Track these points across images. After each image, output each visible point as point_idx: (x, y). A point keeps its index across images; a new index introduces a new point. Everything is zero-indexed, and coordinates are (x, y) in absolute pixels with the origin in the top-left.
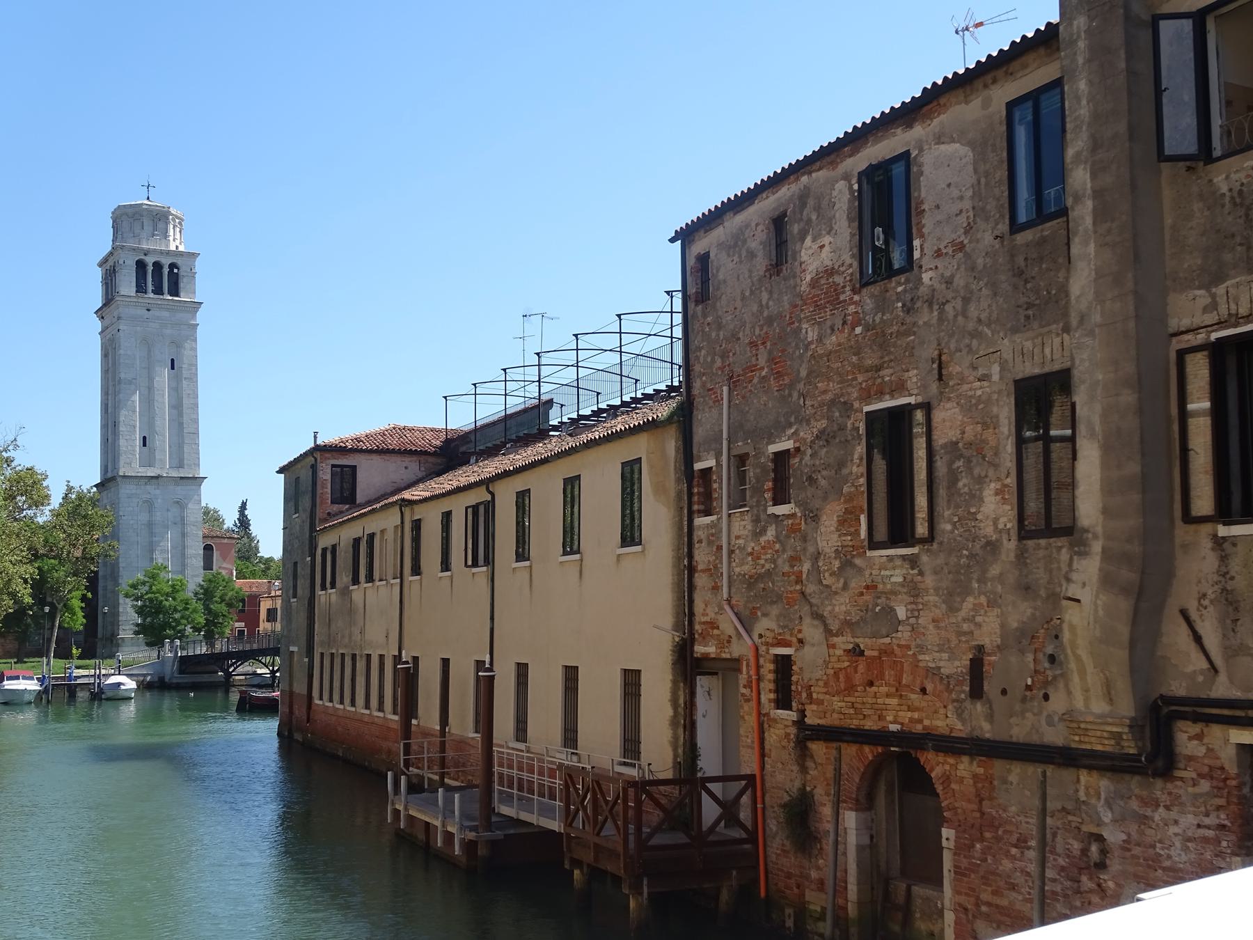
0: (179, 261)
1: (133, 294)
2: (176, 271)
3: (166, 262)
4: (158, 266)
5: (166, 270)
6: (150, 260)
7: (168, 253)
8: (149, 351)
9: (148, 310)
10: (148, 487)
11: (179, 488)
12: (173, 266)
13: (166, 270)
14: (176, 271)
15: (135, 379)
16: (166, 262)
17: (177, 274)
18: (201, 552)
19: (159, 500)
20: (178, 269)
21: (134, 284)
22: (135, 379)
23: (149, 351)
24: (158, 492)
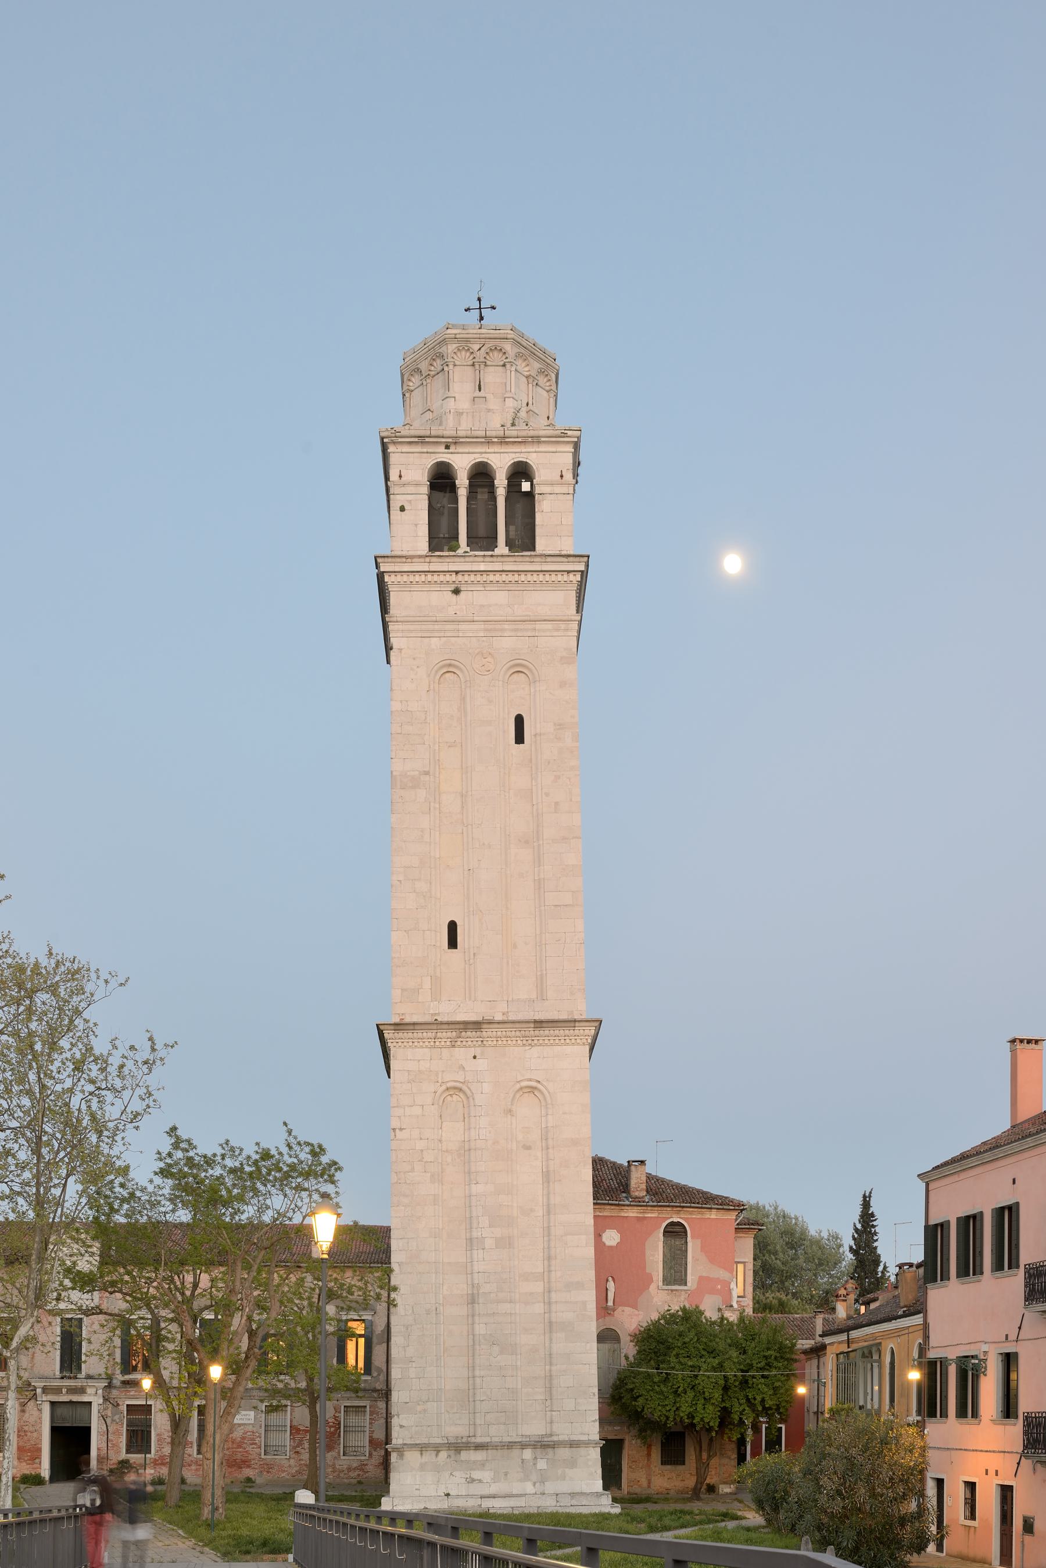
0: (532, 456)
2: (526, 486)
3: (501, 463)
4: (481, 475)
5: (501, 483)
6: (462, 464)
8: (463, 699)
9: (456, 592)
10: (462, 1054)
11: (535, 1051)
12: (520, 472)
13: (501, 483)
15: (427, 773)
16: (501, 463)
17: (530, 495)
18: (592, 1221)
19: (486, 1087)
20: (530, 478)
21: (424, 531)
22: (427, 773)
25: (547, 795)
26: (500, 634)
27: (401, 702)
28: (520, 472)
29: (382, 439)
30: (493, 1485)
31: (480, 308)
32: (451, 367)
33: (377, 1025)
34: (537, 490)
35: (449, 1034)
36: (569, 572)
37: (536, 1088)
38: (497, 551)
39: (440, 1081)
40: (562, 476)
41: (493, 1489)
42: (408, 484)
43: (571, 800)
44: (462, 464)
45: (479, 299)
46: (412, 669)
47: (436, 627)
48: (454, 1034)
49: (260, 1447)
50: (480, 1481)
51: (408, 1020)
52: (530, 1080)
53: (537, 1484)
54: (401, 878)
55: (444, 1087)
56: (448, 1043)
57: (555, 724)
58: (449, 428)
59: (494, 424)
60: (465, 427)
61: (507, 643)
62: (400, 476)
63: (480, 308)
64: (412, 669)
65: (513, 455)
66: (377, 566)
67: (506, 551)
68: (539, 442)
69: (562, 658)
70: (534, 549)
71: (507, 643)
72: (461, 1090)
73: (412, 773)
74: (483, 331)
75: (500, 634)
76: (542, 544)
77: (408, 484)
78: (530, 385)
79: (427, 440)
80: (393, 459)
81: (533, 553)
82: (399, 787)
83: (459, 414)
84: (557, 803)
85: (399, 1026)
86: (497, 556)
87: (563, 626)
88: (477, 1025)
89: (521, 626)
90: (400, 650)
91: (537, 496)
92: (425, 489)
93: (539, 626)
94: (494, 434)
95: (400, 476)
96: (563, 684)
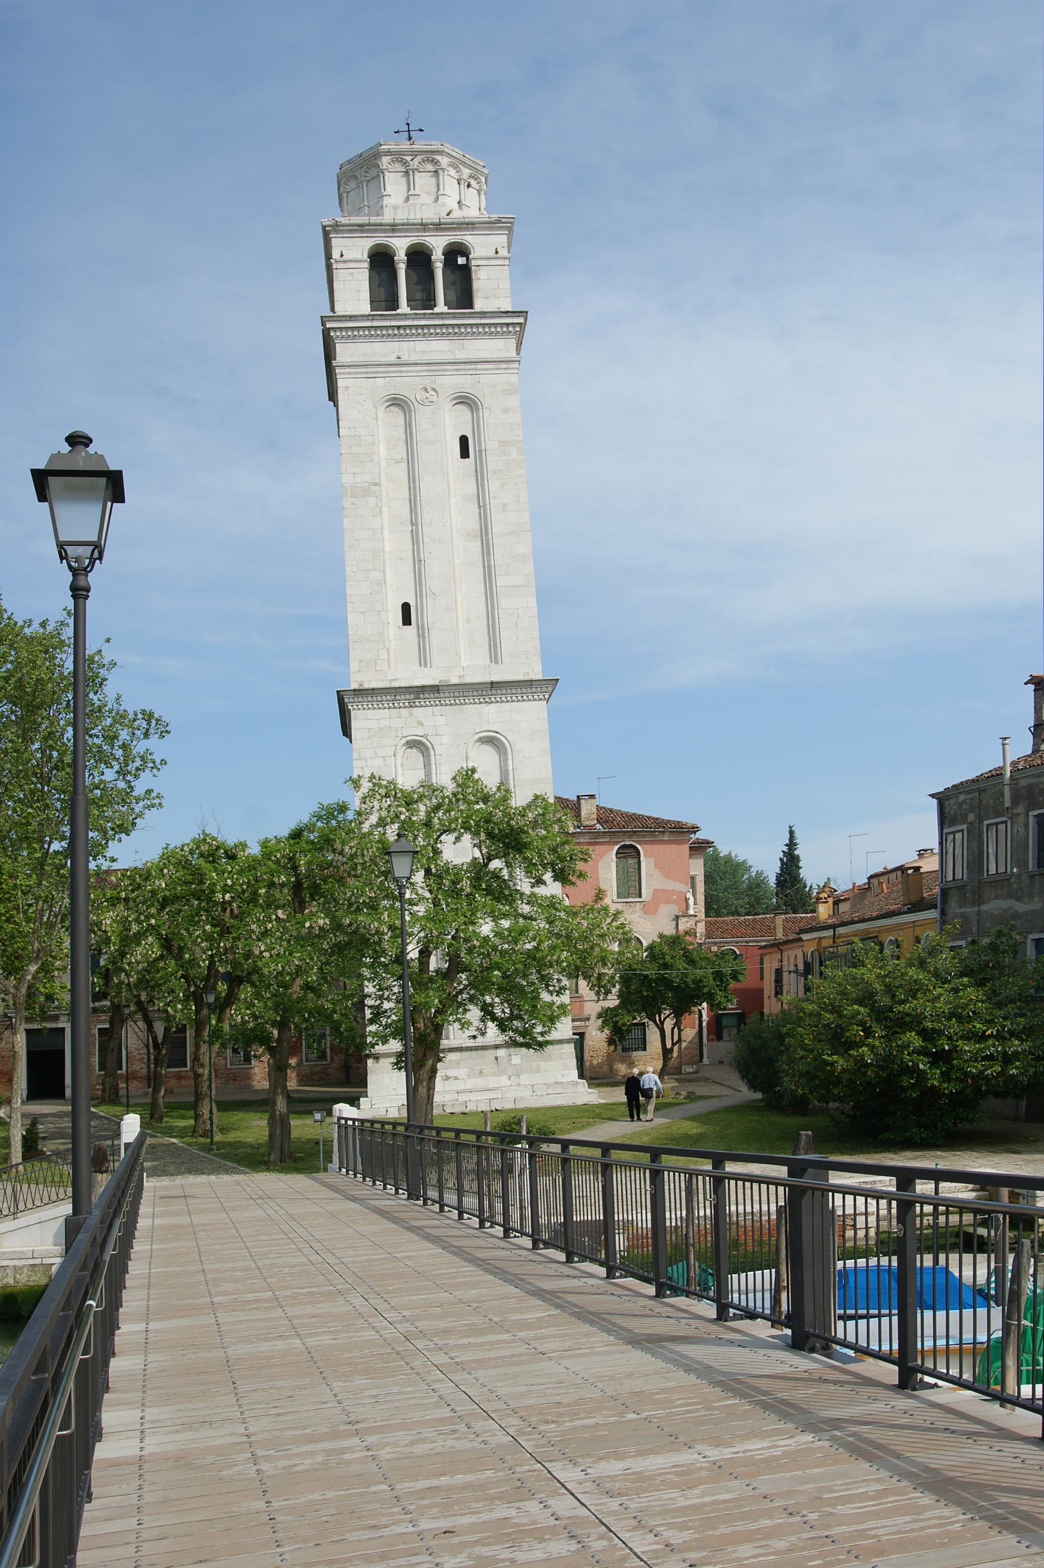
0: (469, 239)
1: (364, 307)
2: (461, 261)
3: (438, 244)
4: (419, 257)
6: (400, 246)
7: (439, 227)
8: (408, 425)
12: (454, 252)
14: (461, 261)
15: (376, 484)
16: (438, 244)
17: (466, 270)
19: (445, 740)
22: (376, 484)
23: (408, 425)
24: (441, 720)
25: (495, 498)
26: (442, 373)
27: (350, 428)
28: (454, 252)
29: (324, 227)
30: (468, 1081)
31: (409, 131)
32: (386, 173)
33: (338, 692)
34: (474, 263)
35: (407, 697)
36: (508, 325)
37: (494, 738)
38: (436, 310)
39: (400, 736)
40: (497, 252)
41: (470, 1084)
42: (350, 261)
43: (518, 501)
44: (400, 246)
45: (408, 124)
46: (359, 403)
47: (380, 369)
48: (412, 696)
49: (226, 1059)
50: (456, 1078)
51: (366, 686)
52: (489, 731)
53: (512, 1078)
54: (355, 569)
55: (404, 741)
56: (407, 704)
57: (499, 442)
58: (387, 217)
59: (430, 214)
60: (401, 217)
61: (451, 382)
62: (342, 255)
63: (409, 131)
64: (359, 403)
65: (449, 238)
66: (323, 324)
67: (445, 309)
68: (474, 229)
69: (504, 390)
70: (470, 305)
71: (451, 382)
72: (420, 742)
73: (363, 485)
74: (413, 146)
75: (442, 373)
76: (479, 305)
77: (350, 261)
78: (462, 186)
79: (366, 228)
80: (335, 242)
81: (471, 311)
82: (350, 495)
83: (395, 208)
84: (504, 505)
85: (359, 692)
86: (437, 314)
87: (504, 366)
88: (435, 689)
89: (463, 367)
90: (347, 388)
91: (473, 268)
92: (366, 265)
93: (479, 366)
94: (429, 221)
95: (342, 255)
96: (506, 411)
